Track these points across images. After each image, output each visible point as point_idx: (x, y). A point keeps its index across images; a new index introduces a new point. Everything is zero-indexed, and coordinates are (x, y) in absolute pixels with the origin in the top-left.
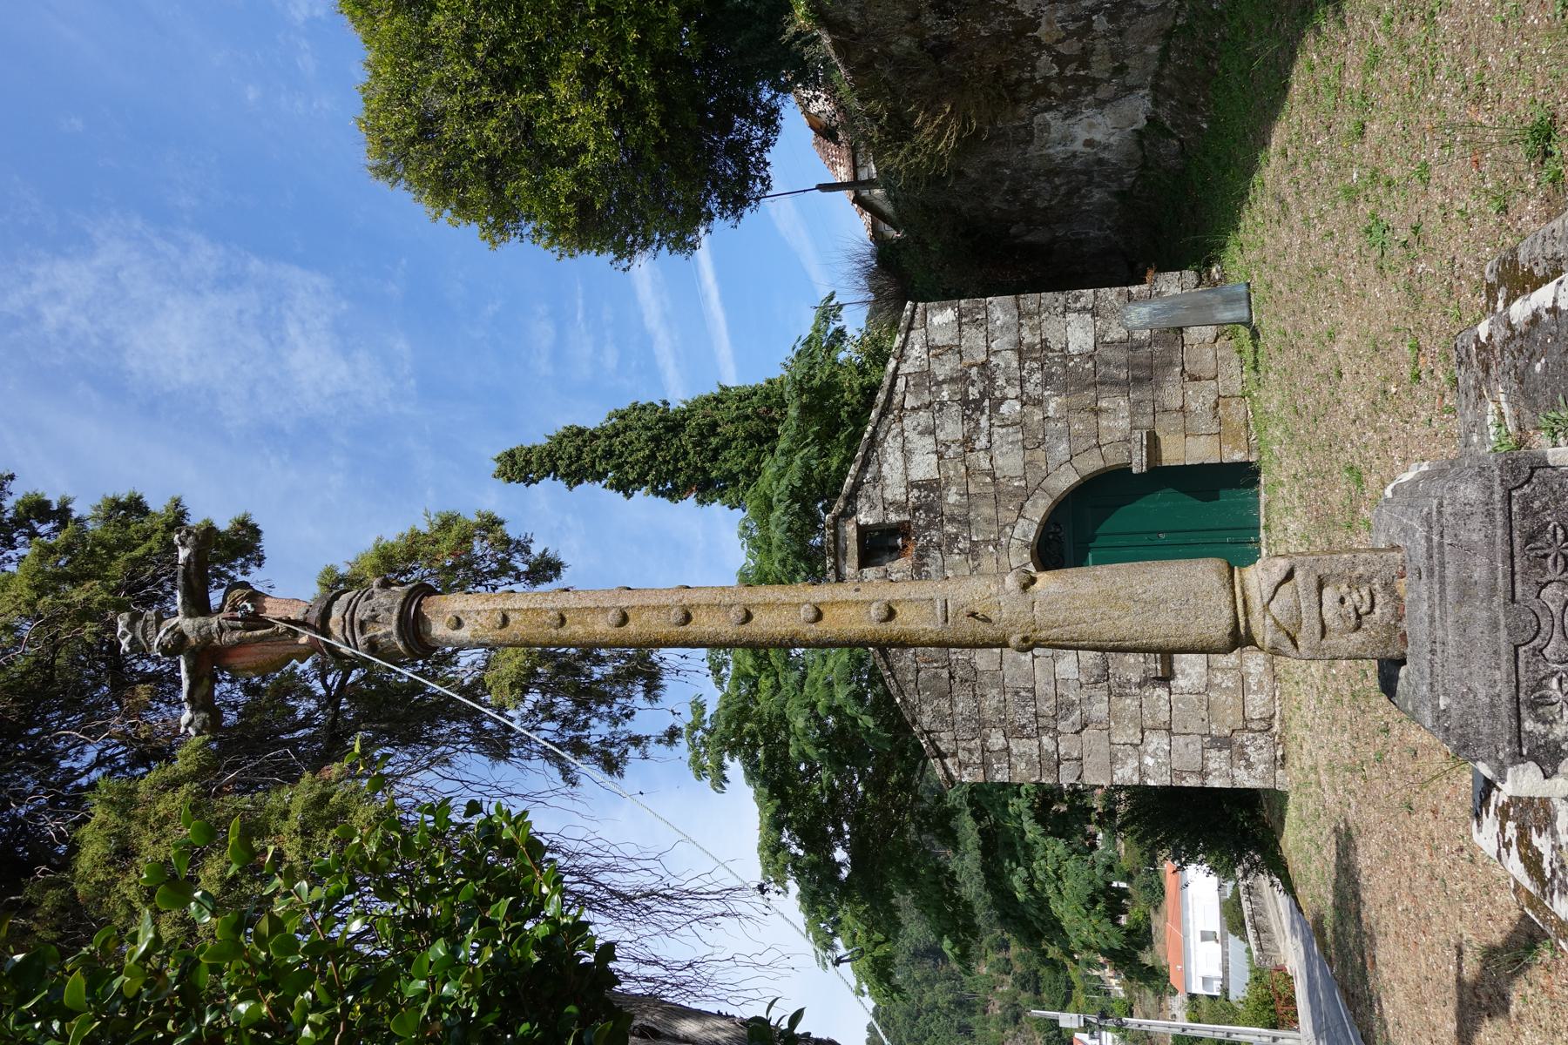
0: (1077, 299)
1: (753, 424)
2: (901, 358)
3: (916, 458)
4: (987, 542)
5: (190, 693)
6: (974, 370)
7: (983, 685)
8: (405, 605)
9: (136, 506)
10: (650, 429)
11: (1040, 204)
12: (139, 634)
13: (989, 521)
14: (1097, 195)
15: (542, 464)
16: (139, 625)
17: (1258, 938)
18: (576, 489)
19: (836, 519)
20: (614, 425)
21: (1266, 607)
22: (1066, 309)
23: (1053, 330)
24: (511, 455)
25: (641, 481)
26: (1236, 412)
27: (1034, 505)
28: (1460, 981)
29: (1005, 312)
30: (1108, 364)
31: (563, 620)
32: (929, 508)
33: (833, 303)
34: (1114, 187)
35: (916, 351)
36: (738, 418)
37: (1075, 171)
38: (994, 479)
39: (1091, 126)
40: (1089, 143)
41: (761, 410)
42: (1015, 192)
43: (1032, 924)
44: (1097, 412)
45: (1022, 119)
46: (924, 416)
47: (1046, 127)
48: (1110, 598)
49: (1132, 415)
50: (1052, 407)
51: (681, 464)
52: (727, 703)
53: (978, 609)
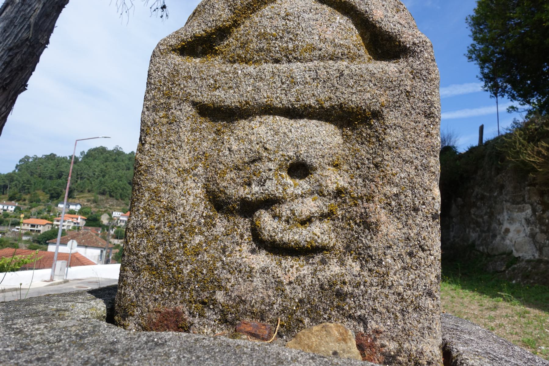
11: (473, 211)
14: (474, 235)
34: (477, 243)
37: (491, 224)
42: (483, 198)
45: (529, 198)
47: (522, 210)
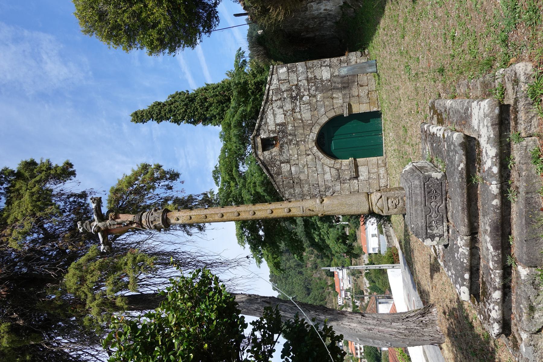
0: (324, 62)
1: (219, 98)
2: (270, 84)
3: (278, 116)
4: (301, 141)
5: (103, 242)
6: (294, 87)
7: (303, 184)
8: (163, 216)
9: (33, 163)
10: (184, 101)
11: (310, 27)
12: (85, 227)
13: (301, 134)
14: (329, 23)
15: (147, 116)
16: (84, 225)
17: (388, 239)
18: (161, 123)
19: (254, 137)
20: (171, 100)
21: (376, 204)
22: (321, 66)
23: (317, 73)
24: (136, 113)
25: (183, 119)
26: (374, 96)
27: (315, 128)
28: (431, 264)
29: (302, 67)
30: (335, 83)
31: (206, 217)
32: (283, 132)
33: (241, 51)
34: (334, 21)
35: (275, 82)
36: (213, 96)
38: (302, 121)
39: (326, 5)
40: (325, 10)
41: (221, 92)
42: (302, 24)
43: (322, 248)
44: (333, 98)
46: (279, 103)
47: (312, 6)
48: (341, 204)
49: (343, 98)
50: (319, 97)
51: (196, 113)
52: (221, 189)
53: (311, 209)
